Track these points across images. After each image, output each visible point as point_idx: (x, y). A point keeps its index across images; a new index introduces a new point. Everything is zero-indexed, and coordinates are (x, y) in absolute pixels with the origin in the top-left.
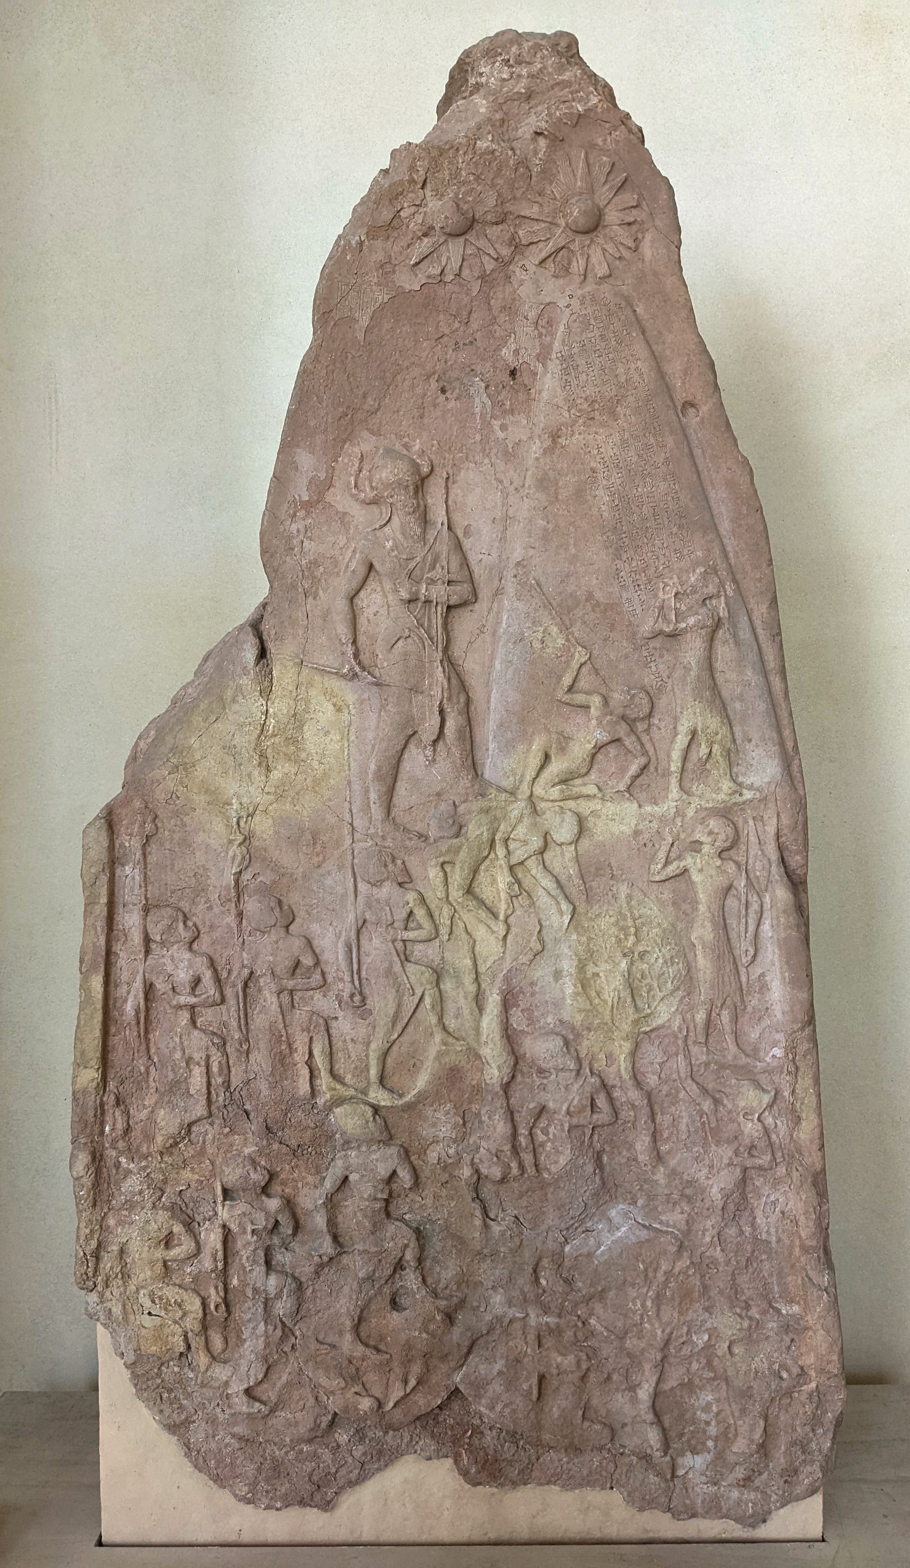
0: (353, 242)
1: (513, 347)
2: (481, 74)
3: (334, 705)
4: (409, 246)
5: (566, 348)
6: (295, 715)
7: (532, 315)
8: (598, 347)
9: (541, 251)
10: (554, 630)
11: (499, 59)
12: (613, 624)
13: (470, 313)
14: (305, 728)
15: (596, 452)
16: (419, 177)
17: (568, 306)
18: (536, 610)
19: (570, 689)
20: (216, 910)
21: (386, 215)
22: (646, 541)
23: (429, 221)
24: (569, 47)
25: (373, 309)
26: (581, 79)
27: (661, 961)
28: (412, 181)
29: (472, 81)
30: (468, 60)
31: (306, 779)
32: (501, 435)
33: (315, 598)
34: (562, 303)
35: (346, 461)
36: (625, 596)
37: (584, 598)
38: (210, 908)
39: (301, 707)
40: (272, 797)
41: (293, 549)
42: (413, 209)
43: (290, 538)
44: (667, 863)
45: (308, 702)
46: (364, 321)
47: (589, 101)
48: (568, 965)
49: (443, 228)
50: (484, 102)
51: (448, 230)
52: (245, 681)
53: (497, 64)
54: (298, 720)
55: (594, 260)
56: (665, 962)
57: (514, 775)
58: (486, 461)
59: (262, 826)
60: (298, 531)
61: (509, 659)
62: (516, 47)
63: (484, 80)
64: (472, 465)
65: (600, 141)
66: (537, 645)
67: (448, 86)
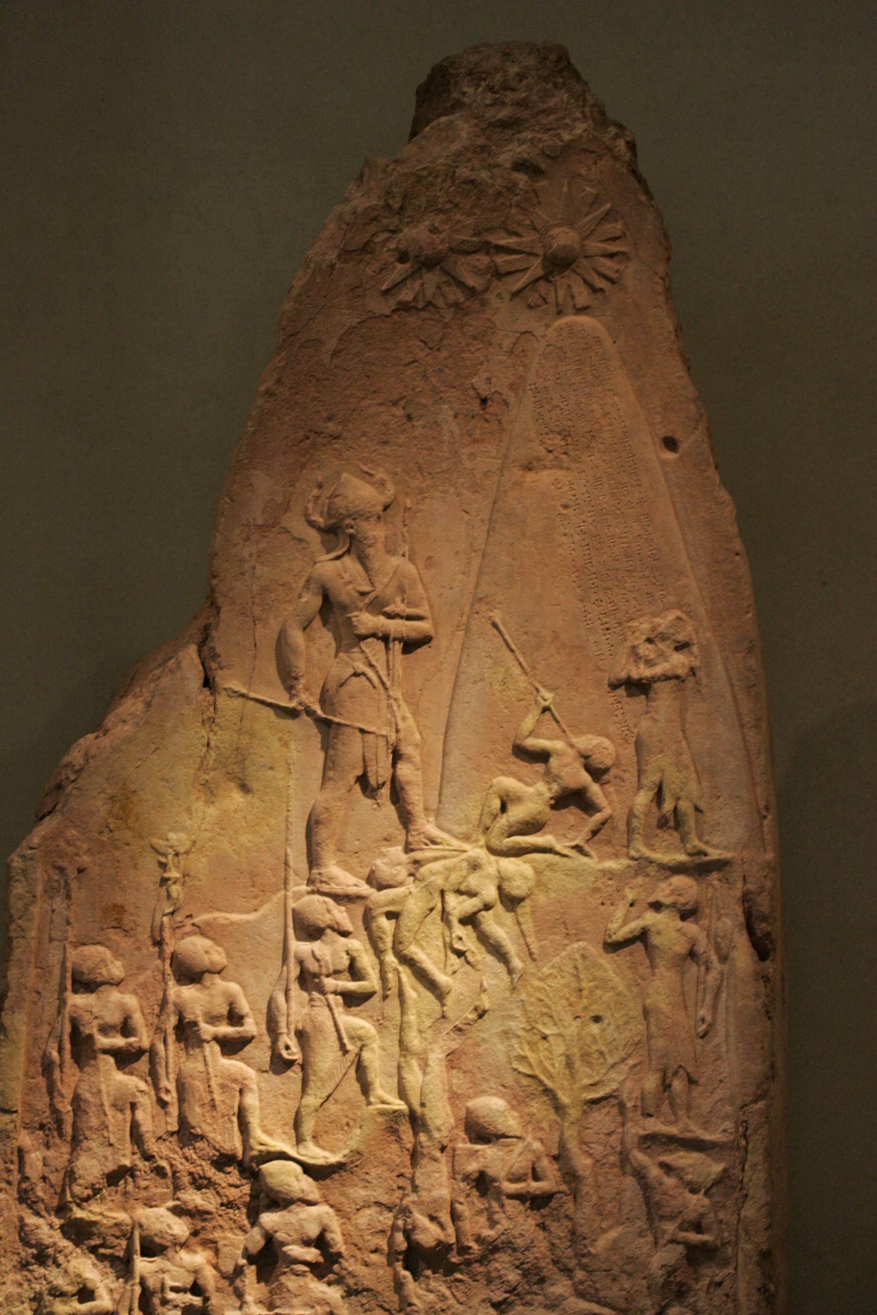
0: (324, 266)
1: (486, 375)
2: (464, 93)
3: (280, 740)
4: (381, 270)
5: (541, 380)
6: (237, 749)
7: (507, 343)
8: (573, 381)
9: (518, 281)
10: (517, 671)
11: (483, 84)
12: (579, 669)
13: (442, 340)
14: (247, 762)
15: (566, 488)
16: (396, 206)
17: (544, 336)
18: (498, 650)
19: (531, 734)
20: (144, 951)
21: (360, 239)
22: (616, 583)
23: (402, 246)
24: (559, 60)
25: (341, 332)
26: (568, 103)
27: (612, 1027)
28: (387, 207)
29: (455, 95)
30: (451, 71)
31: (245, 818)
32: (468, 464)
33: (264, 627)
34: (539, 333)
35: (304, 486)
36: (592, 638)
37: (549, 639)
38: (138, 948)
39: (244, 740)
40: (208, 834)
41: (243, 574)
42: (386, 235)
43: (242, 561)
44: (625, 923)
45: (252, 734)
46: (332, 344)
47: (574, 128)
48: (517, 1025)
49: (417, 257)
50: (466, 126)
51: (422, 259)
52: (186, 710)
53: (480, 89)
54: (241, 756)
55: (575, 290)
56: (618, 1027)
57: (468, 822)
58: (452, 490)
59: (199, 864)
60: (251, 555)
61: (466, 700)
62: (500, 74)
63: (466, 100)
64: (439, 494)
65: (583, 171)
66: (497, 687)
67: (431, 78)
